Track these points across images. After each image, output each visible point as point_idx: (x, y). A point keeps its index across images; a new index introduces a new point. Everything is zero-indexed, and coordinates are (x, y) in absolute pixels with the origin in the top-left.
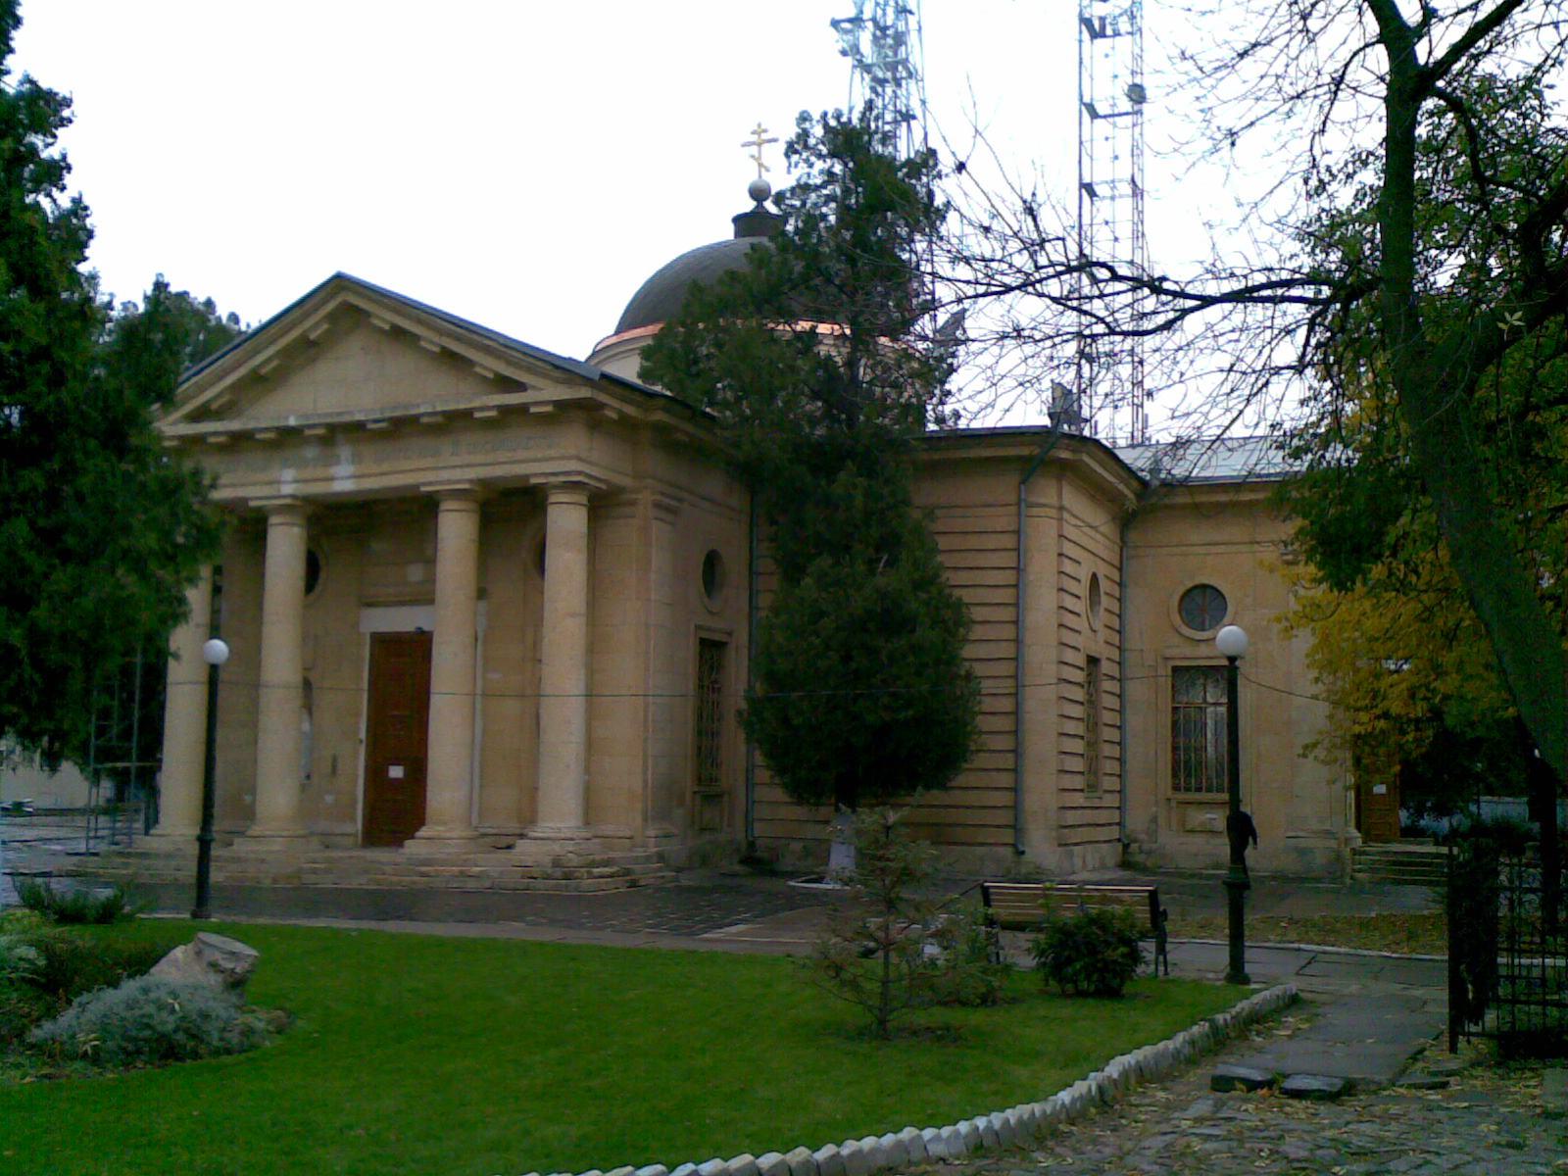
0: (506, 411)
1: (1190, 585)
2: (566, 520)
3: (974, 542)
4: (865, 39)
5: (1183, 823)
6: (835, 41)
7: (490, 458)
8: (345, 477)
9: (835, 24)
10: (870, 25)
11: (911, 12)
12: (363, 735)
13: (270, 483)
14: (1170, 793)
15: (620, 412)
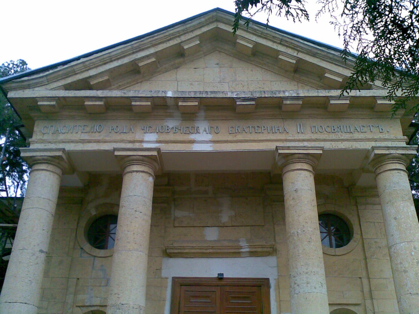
7: (333, 136)
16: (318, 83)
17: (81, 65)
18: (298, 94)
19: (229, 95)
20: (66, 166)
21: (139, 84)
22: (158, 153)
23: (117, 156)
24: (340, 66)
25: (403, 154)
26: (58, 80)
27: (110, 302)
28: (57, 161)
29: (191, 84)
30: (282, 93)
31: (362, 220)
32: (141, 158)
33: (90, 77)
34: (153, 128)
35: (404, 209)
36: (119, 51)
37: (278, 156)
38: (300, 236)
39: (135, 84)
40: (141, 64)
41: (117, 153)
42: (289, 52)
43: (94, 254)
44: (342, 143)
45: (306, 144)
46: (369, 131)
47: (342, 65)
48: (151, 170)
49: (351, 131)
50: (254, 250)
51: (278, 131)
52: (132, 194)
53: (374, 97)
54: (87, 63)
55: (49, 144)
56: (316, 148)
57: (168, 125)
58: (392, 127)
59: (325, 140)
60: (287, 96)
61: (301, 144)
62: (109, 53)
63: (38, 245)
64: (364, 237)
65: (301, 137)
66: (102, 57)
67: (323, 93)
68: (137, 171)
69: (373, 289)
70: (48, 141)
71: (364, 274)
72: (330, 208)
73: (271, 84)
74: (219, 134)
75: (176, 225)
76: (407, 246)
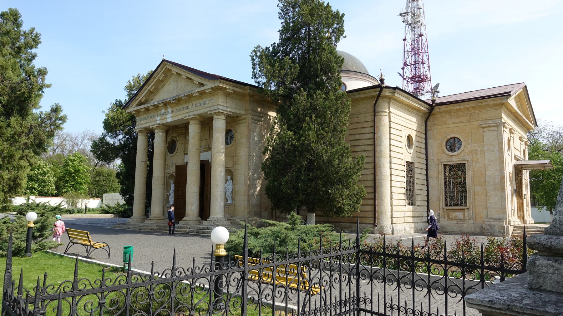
0: (202, 93)
1: (449, 137)
2: (220, 125)
3: (360, 125)
4: (409, 18)
5: (448, 216)
6: (401, 19)
8: (169, 119)
9: (401, 15)
10: (410, 13)
11: (421, 8)
13: (155, 121)
14: (444, 207)
15: (234, 90)
33: (141, 100)
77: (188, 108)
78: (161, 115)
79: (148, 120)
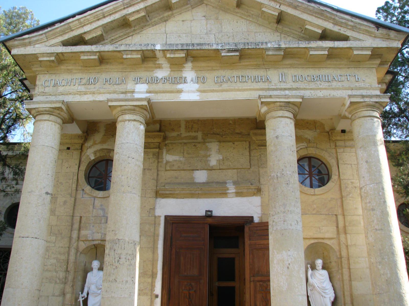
12: (158, 290)
13: (125, 93)
16: (300, 34)
17: (77, 22)
18: (279, 45)
19: (214, 47)
20: (66, 116)
21: (130, 38)
22: (149, 103)
23: (110, 106)
24: (319, 18)
25: (376, 102)
26: (56, 37)
27: (108, 238)
28: (58, 112)
29: (179, 36)
30: (264, 44)
31: (340, 162)
32: (132, 107)
33: (85, 33)
34: (143, 79)
35: (375, 153)
36: (112, 7)
37: (261, 104)
38: (279, 179)
39: (126, 38)
40: (131, 19)
41: (110, 104)
42: (271, 5)
43: (94, 195)
44: (321, 91)
45: (287, 92)
46: (346, 80)
47: (321, 17)
48: (142, 118)
49: (330, 80)
50: (240, 191)
51: (261, 80)
52: (125, 142)
53: (350, 48)
54: (82, 20)
55: (50, 96)
56: (297, 97)
57: (157, 76)
58: (367, 76)
59: (305, 89)
60: (269, 47)
61: (283, 93)
62: (102, 10)
63: (44, 188)
64: (341, 178)
65: (283, 86)
66: (95, 14)
67: (303, 45)
68: (129, 121)
69: (347, 224)
70: (49, 94)
71: (340, 211)
72: (312, 152)
73: (255, 36)
74: (205, 84)
75: (168, 168)
76: (376, 187)
77: (268, 80)
78: (153, 81)
79: (92, 86)
